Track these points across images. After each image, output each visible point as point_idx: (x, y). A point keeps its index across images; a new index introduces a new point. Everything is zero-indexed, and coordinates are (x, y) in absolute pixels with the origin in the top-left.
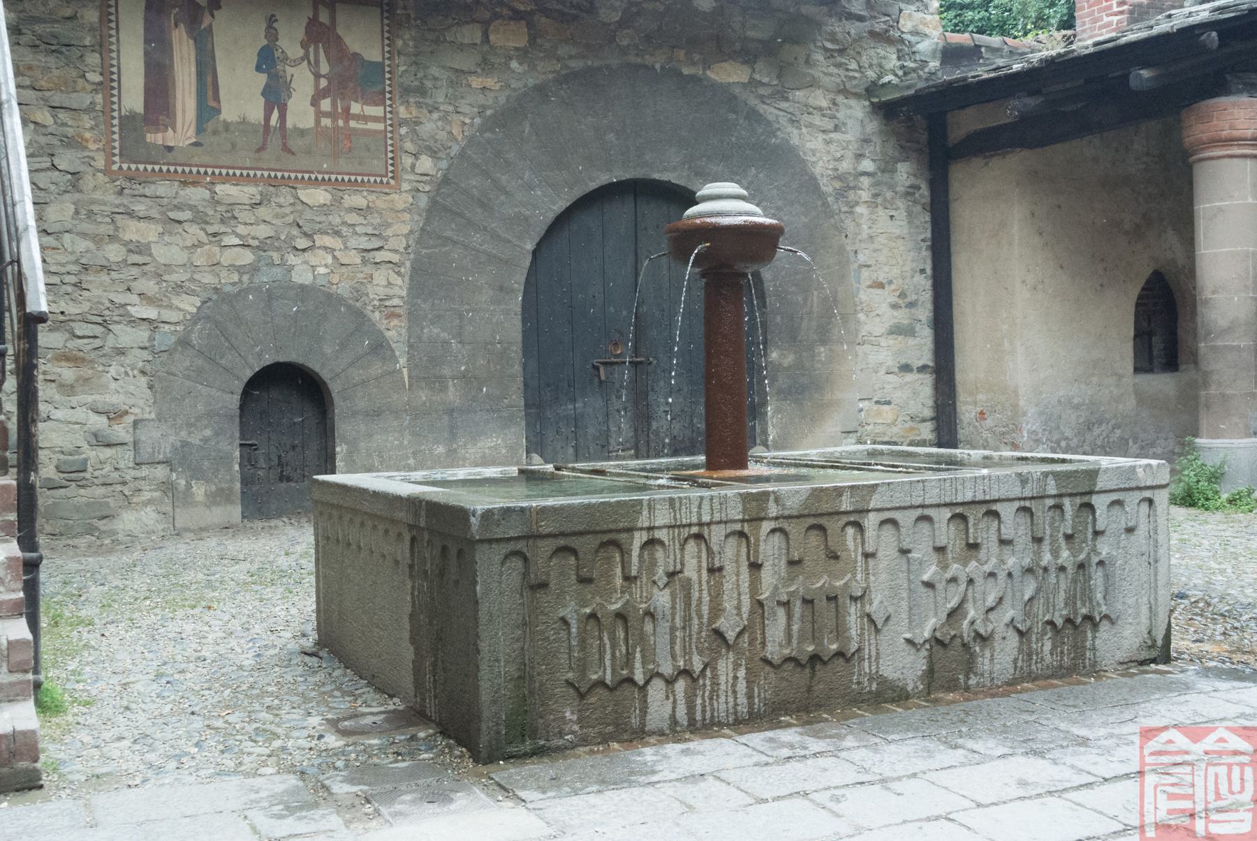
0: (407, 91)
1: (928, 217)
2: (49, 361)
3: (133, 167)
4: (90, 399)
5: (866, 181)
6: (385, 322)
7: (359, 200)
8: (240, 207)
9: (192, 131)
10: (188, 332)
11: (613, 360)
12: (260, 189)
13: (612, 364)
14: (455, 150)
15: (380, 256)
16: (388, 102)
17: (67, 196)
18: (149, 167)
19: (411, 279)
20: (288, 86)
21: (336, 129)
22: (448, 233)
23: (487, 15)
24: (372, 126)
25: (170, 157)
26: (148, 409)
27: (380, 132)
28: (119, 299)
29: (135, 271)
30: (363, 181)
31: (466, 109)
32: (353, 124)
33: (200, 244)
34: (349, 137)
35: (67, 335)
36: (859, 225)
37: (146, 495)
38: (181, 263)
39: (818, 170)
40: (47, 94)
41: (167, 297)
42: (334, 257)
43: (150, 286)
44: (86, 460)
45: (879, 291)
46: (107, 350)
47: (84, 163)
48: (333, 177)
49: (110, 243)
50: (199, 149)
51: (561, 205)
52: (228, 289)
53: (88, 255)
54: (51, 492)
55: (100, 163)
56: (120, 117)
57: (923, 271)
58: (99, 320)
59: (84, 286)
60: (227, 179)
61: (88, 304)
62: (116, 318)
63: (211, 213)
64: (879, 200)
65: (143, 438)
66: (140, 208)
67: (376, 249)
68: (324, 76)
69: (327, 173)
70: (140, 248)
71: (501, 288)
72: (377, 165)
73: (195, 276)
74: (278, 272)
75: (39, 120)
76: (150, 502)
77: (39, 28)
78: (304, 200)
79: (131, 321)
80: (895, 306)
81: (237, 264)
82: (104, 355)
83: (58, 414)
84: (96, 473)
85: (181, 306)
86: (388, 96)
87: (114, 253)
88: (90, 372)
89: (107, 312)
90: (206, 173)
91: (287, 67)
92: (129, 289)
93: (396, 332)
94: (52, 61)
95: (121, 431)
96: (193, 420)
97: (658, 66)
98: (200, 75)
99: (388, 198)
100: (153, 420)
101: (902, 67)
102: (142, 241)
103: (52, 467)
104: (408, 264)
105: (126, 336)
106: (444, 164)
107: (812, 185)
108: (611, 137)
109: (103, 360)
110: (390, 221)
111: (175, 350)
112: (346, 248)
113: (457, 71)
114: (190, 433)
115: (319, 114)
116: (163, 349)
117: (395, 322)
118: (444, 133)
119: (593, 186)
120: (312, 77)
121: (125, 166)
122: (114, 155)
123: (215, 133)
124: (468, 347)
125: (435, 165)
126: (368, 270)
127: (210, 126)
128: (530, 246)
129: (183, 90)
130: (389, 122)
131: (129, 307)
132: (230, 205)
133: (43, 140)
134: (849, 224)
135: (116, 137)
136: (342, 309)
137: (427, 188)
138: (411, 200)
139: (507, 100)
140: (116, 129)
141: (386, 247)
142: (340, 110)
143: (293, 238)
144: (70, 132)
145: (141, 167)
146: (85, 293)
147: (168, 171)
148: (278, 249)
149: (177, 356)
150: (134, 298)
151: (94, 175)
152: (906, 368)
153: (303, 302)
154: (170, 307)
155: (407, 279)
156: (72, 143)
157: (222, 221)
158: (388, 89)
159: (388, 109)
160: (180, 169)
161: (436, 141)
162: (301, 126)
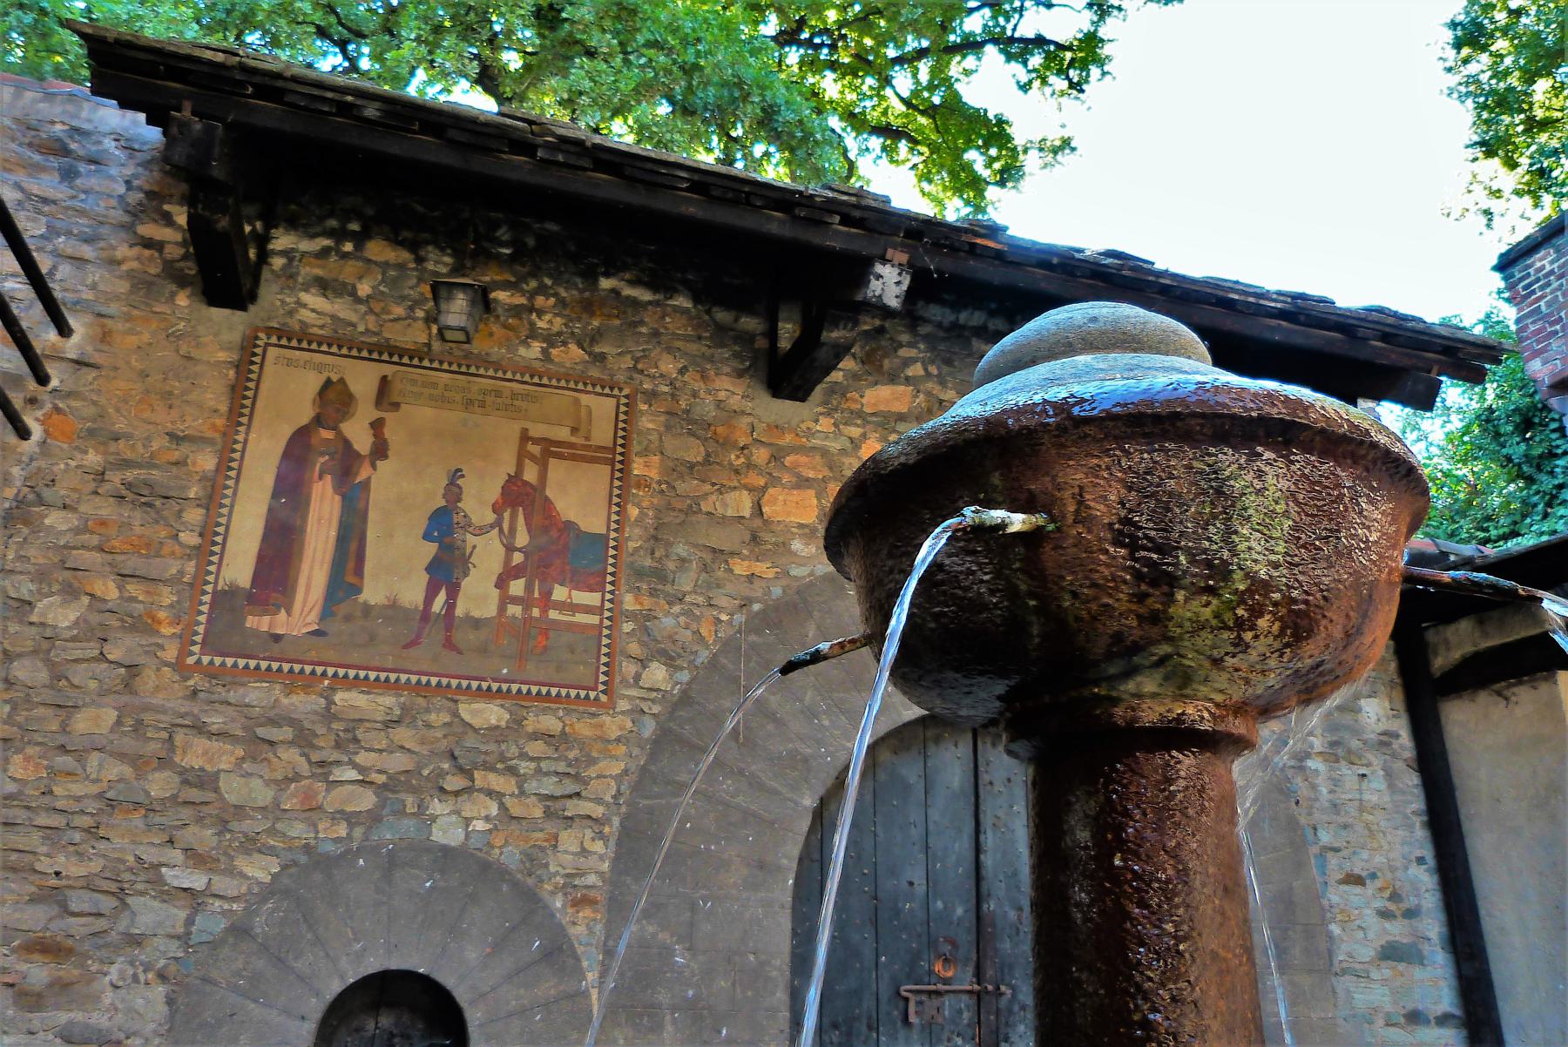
2: (14, 951)
3: (218, 660)
4: (63, 1017)
6: (570, 910)
8: (368, 725)
9: (313, 617)
10: (249, 913)
11: (940, 987)
12: (402, 699)
13: (938, 993)
14: (703, 656)
15: (573, 808)
16: (609, 587)
17: (109, 699)
18: (241, 662)
19: (619, 844)
21: (528, 620)
24: (581, 618)
25: (276, 649)
27: (593, 626)
28: (150, 855)
29: (186, 813)
30: (558, 695)
31: (723, 601)
33: (297, 777)
34: (545, 633)
35: (55, 910)
36: (1314, 787)
38: (261, 804)
40: (119, 558)
42: (502, 806)
45: (1358, 889)
46: (114, 936)
47: (146, 652)
48: (515, 687)
49: (159, 769)
50: (320, 640)
52: (330, 848)
53: (121, 786)
55: (171, 654)
56: (215, 592)
57: (1421, 861)
58: (113, 887)
59: (102, 833)
60: (356, 683)
61: (102, 862)
62: (140, 887)
63: (321, 730)
64: (1340, 752)
67: (570, 797)
68: (519, 550)
69: (506, 681)
70: (206, 780)
71: (762, 866)
73: (279, 826)
74: (408, 826)
75: (99, 593)
77: (131, 475)
78: (466, 717)
79: (163, 892)
80: (1385, 914)
81: (348, 809)
82: (106, 945)
85: (249, 871)
86: (610, 578)
87: (159, 785)
88: (76, 972)
89: (127, 876)
90: (324, 674)
91: (469, 536)
92: (171, 842)
93: (583, 928)
94: (138, 515)
98: (342, 540)
99: (594, 721)
102: (208, 768)
104: (616, 821)
105: (148, 913)
106: (684, 676)
109: (104, 953)
110: (595, 754)
112: (522, 793)
113: (714, 550)
115: (505, 600)
117: (586, 912)
118: (688, 633)
120: (502, 550)
121: (206, 659)
123: (348, 618)
124: (701, 958)
125: (671, 676)
126: (550, 827)
127: (343, 609)
129: (313, 562)
130: (607, 614)
131: (164, 870)
132: (354, 720)
133: (95, 618)
135: (202, 618)
136: (505, 888)
137: (656, 709)
138: (629, 724)
139: (784, 591)
140: (205, 608)
141: (583, 794)
142: (536, 595)
143: (442, 774)
144: (139, 608)
145: (230, 661)
146: (102, 845)
148: (414, 790)
149: (225, 951)
150: (176, 855)
151: (158, 670)
152: (1415, 1018)
153: (442, 872)
154: (231, 872)
155: (612, 843)
156: (143, 625)
157: (338, 745)
158: (610, 569)
159: (608, 596)
160: (286, 667)
161: (674, 642)
162: (476, 614)
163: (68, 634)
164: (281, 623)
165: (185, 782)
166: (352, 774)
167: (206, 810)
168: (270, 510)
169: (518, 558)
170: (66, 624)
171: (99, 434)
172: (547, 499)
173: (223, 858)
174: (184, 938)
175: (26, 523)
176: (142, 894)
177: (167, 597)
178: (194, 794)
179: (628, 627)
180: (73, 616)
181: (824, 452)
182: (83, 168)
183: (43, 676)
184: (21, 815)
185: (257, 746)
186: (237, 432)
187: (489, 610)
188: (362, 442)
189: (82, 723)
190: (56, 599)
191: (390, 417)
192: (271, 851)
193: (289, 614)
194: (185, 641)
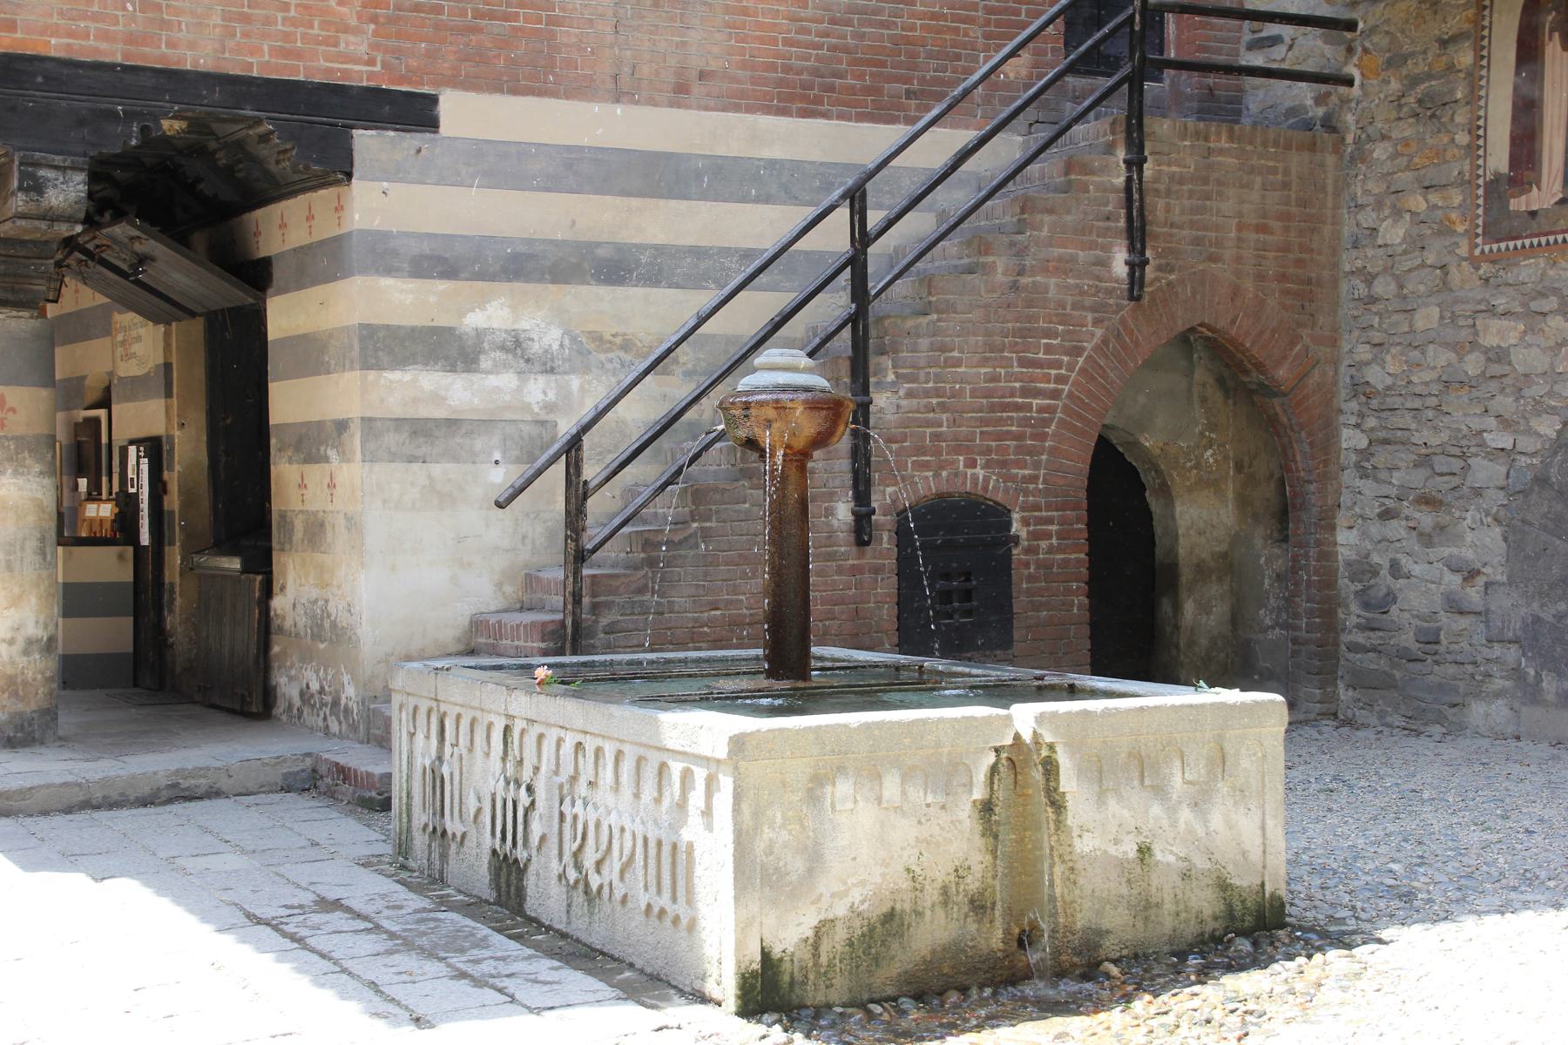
3: (1495, 247)
4: (1446, 551)
10: (1546, 465)
17: (1433, 300)
18: (1511, 244)
26: (1500, 569)
28: (1476, 424)
29: (1493, 386)
37: (1499, 683)
40: (1422, 172)
41: (1524, 418)
43: (1504, 404)
44: (1439, 629)
47: (1449, 252)
49: (1471, 351)
53: (1450, 369)
54: (1411, 664)
55: (1463, 250)
56: (1486, 183)
58: (1457, 451)
59: (1444, 409)
62: (1473, 450)
65: (1493, 608)
73: (1556, 388)
76: (1499, 694)
79: (1488, 453)
82: (1461, 497)
84: (1453, 647)
85: (1542, 430)
88: (1448, 518)
89: (1464, 442)
95: (1474, 595)
96: (1546, 587)
100: (1504, 584)
102: (1502, 344)
103: (1411, 634)
111: (1532, 490)
114: (1542, 605)
116: (1517, 489)
121: (1487, 248)
122: (1477, 235)
131: (1485, 434)
135: (1480, 211)
140: (1480, 201)
145: (1503, 245)
146: (1446, 419)
147: (1532, 245)
149: (1534, 498)
150: (1491, 422)
151: (1459, 265)
154: (1529, 432)
156: (1445, 230)
163: (1400, 250)
165: (1489, 359)
167: (1505, 381)
168: (1516, 88)
170: (1398, 240)
173: (1522, 421)
175: (1363, 161)
176: (1476, 455)
178: (1496, 369)
180: (1401, 232)
183: (1393, 287)
184: (1396, 402)
186: (1483, 18)
189: (1420, 323)
190: (1390, 221)
192: (1552, 411)
193: (1539, 189)
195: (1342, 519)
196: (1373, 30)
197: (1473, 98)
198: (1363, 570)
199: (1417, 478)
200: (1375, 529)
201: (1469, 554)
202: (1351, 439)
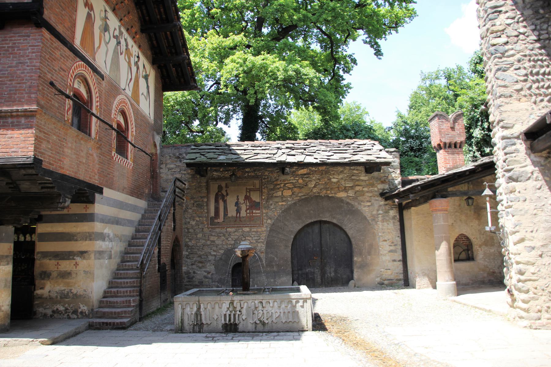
0: (265, 208)
1: (399, 223)
4: (204, 269)
5: (380, 216)
7: (255, 230)
9: (223, 219)
14: (276, 218)
15: (259, 241)
20: (241, 209)
21: (250, 216)
22: (274, 235)
23: (283, 190)
24: (257, 215)
28: (209, 251)
29: (212, 246)
32: (254, 215)
34: (253, 217)
36: (379, 227)
39: (366, 215)
43: (215, 248)
51: (300, 227)
55: (206, 226)
57: (398, 237)
66: (213, 234)
70: (214, 241)
71: (286, 246)
72: (258, 222)
80: (390, 246)
83: (199, 272)
87: (209, 243)
93: (263, 256)
95: (209, 276)
97: (323, 195)
101: (390, 188)
106: (273, 221)
107: (365, 218)
108: (312, 212)
115: (247, 213)
117: (263, 254)
119: (307, 223)
127: (226, 218)
128: (293, 237)
134: (376, 227)
148: (239, 240)
150: (212, 251)
152: (394, 261)
154: (219, 252)
156: (202, 223)
164: (219, 221)
166: (231, 239)
169: (248, 207)
171: (192, 198)
172: (251, 198)
174: (215, 260)
177: (205, 219)
178: (213, 243)
179: (264, 215)
181: (292, 183)
182: (182, 160)
183: (193, 231)
185: (219, 237)
187: (245, 215)
188: (225, 194)
191: (227, 189)
192: (223, 249)
194: (208, 224)
195: (183, 265)
196: (188, 193)
197: (207, 205)
198: (188, 273)
199: (199, 259)
200: (190, 267)
201: (208, 270)
202: (185, 253)
